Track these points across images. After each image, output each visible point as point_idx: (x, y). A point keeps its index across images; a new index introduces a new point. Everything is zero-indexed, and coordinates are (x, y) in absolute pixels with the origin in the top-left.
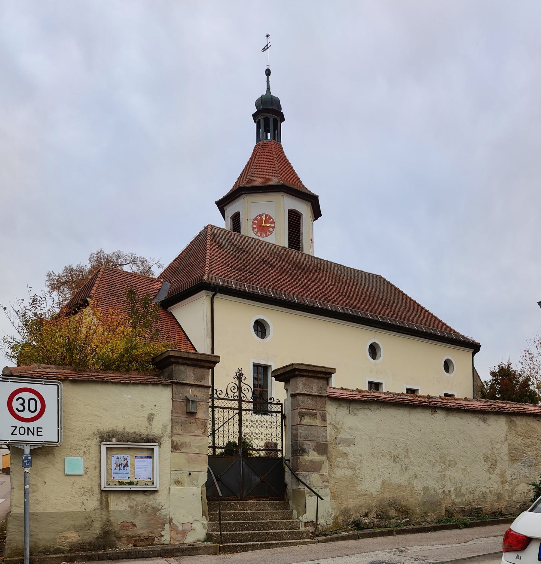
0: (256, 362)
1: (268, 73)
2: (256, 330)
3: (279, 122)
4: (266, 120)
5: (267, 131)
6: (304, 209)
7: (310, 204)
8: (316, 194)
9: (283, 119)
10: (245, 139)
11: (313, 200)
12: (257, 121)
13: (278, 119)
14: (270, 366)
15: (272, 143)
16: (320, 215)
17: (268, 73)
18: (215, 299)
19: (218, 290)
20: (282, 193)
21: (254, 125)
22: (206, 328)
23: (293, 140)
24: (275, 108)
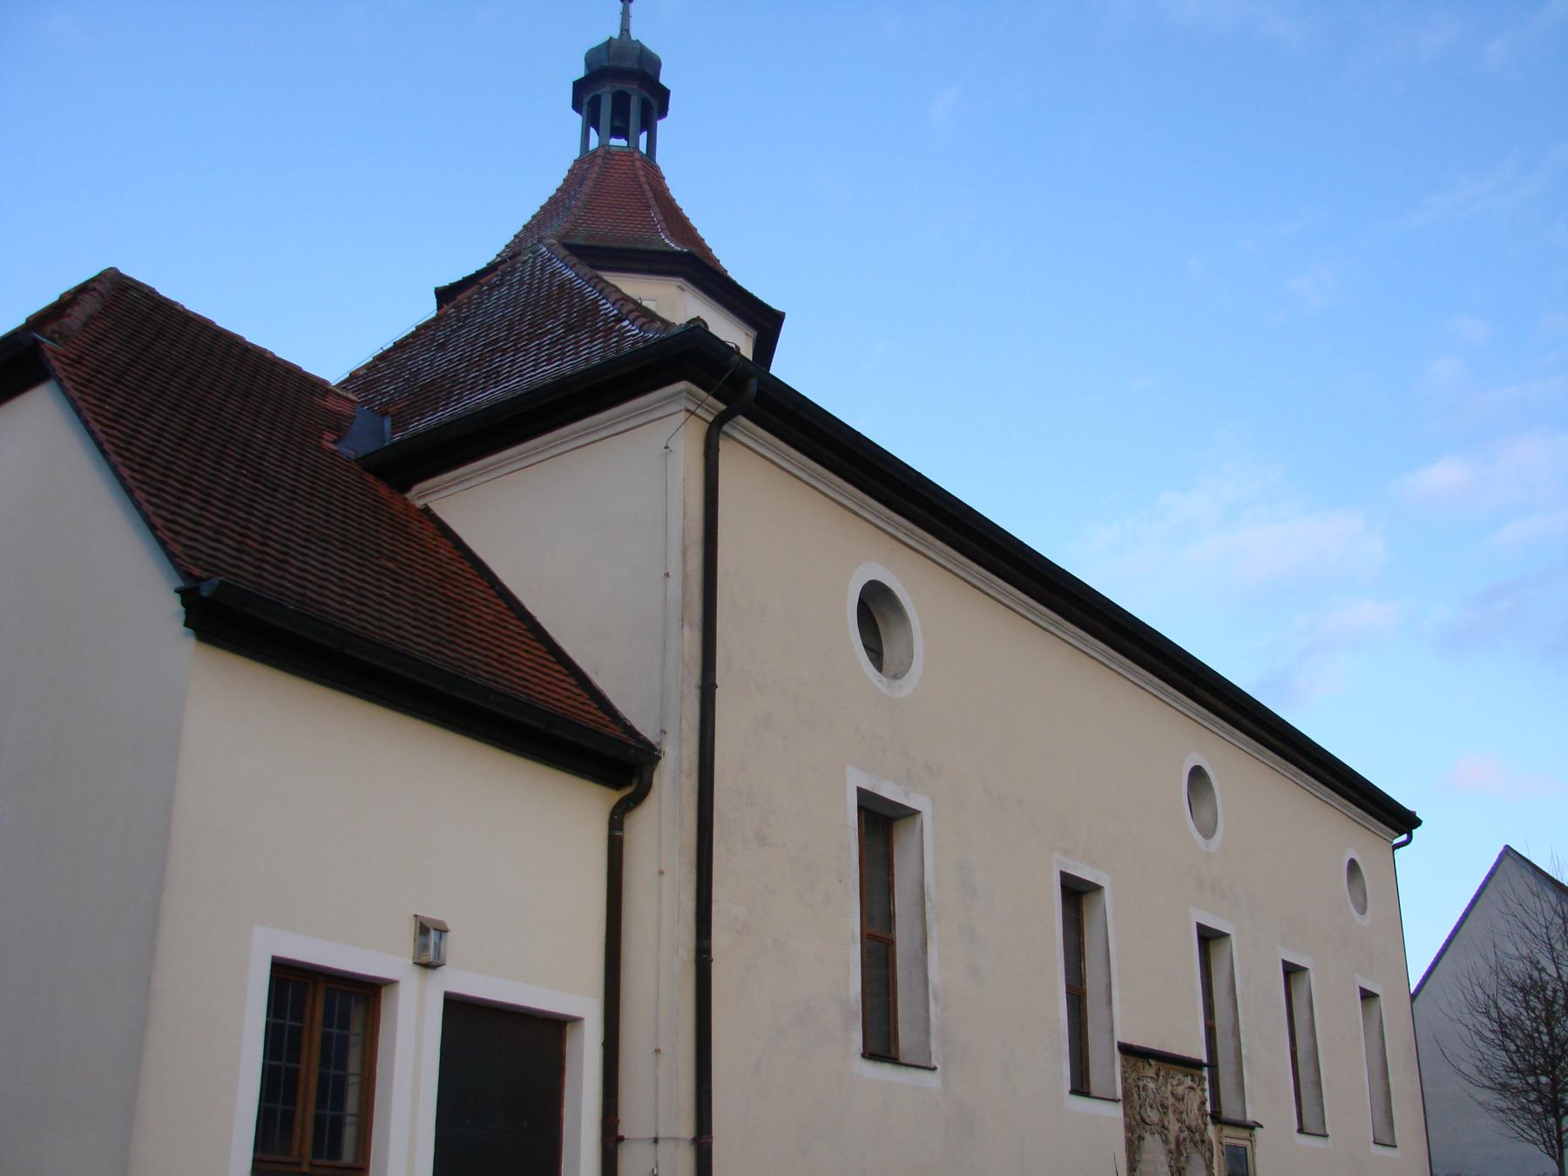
3: (655, 113)
4: (621, 105)
7: (753, 334)
8: (776, 305)
9: (663, 113)
12: (586, 100)
13: (655, 103)
14: (913, 813)
20: (680, 281)
24: (650, 71)
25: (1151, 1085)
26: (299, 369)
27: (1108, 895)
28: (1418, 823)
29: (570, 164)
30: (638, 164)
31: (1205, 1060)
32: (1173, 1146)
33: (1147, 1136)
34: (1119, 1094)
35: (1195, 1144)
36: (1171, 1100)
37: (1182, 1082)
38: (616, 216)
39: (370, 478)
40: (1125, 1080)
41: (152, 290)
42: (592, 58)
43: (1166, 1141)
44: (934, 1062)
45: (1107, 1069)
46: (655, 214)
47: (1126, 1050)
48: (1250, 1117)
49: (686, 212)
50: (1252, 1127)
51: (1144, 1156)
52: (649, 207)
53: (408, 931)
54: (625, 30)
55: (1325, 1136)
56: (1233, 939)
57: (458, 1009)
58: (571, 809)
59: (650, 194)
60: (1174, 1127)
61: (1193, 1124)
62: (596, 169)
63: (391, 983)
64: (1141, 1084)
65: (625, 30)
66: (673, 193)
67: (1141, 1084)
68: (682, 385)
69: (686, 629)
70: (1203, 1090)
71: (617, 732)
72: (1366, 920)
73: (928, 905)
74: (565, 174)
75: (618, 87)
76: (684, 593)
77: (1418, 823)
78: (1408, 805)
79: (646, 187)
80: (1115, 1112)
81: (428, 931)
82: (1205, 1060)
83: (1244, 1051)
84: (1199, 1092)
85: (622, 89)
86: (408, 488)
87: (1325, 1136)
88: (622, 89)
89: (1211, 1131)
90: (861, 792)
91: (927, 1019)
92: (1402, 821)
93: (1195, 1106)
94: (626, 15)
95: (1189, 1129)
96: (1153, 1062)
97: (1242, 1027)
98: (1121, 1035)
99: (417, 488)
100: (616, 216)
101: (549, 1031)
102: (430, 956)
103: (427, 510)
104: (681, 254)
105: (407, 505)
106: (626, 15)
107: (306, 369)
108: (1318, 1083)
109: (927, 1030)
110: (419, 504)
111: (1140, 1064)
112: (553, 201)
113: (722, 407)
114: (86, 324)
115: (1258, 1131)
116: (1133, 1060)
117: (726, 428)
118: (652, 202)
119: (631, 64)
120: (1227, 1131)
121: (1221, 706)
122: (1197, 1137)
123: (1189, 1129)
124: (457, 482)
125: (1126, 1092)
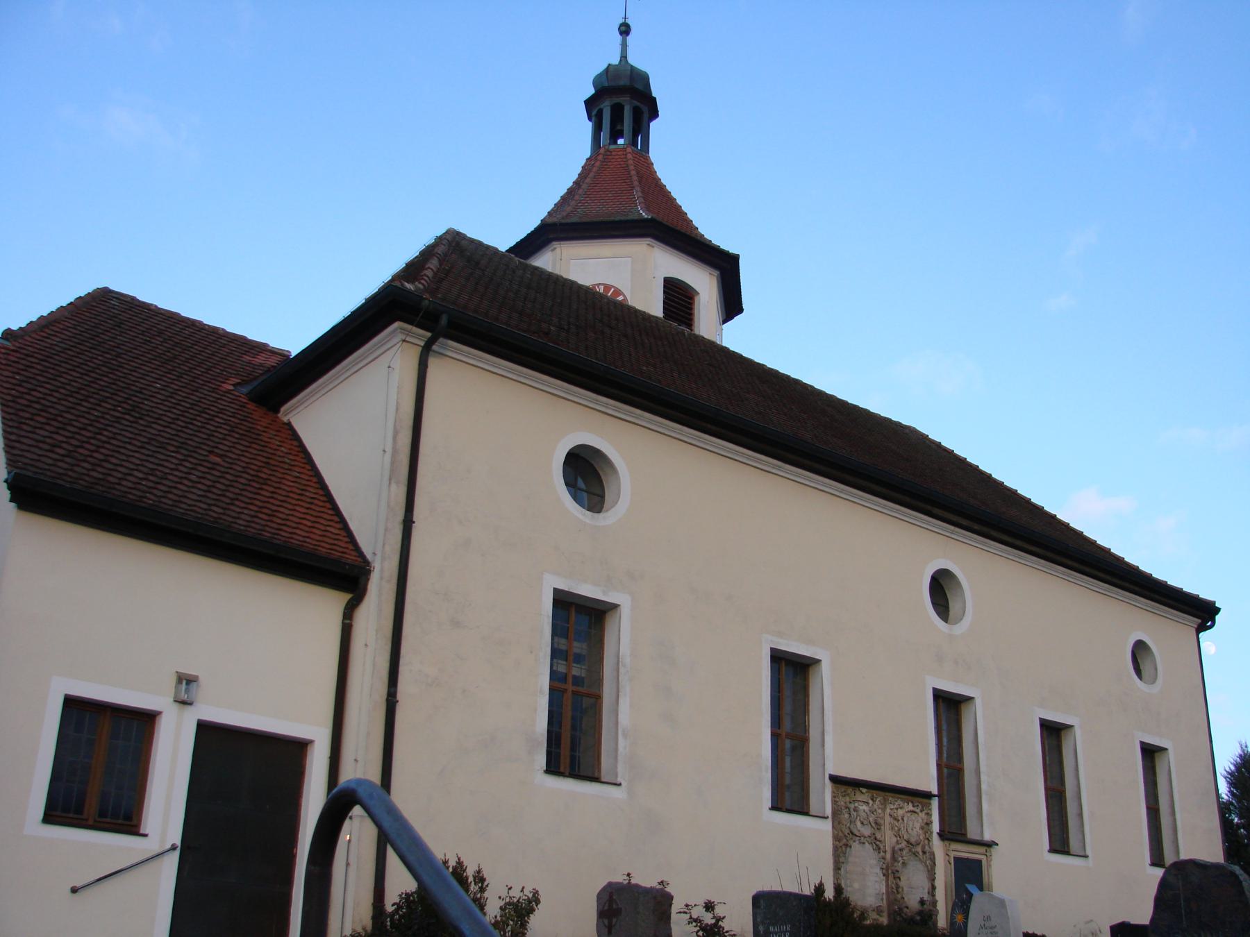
0: (563, 586)
1: (625, 30)
2: (570, 484)
3: (646, 116)
4: (617, 112)
5: (615, 134)
6: (703, 282)
7: (716, 273)
8: (733, 251)
9: (654, 114)
10: (570, 146)
11: (726, 267)
12: (594, 113)
13: (645, 109)
14: (615, 607)
15: (629, 150)
16: (740, 310)
17: (625, 30)
18: (434, 365)
19: (444, 320)
20: (648, 241)
21: (589, 126)
22: (389, 449)
23: (678, 157)
24: (639, 86)
25: (864, 807)
26: (245, 338)
27: (825, 667)
28: (1217, 610)
29: (583, 162)
30: (629, 156)
31: (935, 791)
32: (888, 856)
33: (856, 846)
34: (829, 812)
35: (915, 854)
36: (888, 819)
37: (904, 808)
38: (621, 196)
39: (252, 406)
40: (834, 802)
41: (133, 299)
42: (595, 83)
43: (878, 849)
44: (619, 780)
45: (822, 795)
46: (637, 193)
47: (835, 780)
48: (987, 837)
49: (668, 188)
50: (990, 845)
51: (850, 859)
52: (633, 188)
53: (174, 679)
54: (624, 57)
55: (1086, 857)
56: (978, 702)
57: (204, 729)
58: (319, 608)
59: (635, 178)
60: (889, 839)
61: (913, 840)
62: (598, 164)
63: (159, 713)
64: (852, 806)
65: (624, 57)
66: (659, 174)
67: (852, 806)
68: (396, 325)
69: (394, 486)
70: (929, 815)
71: (351, 557)
72: (1156, 689)
73: (622, 670)
74: (579, 170)
75: (616, 100)
76: (393, 463)
77: (1217, 610)
78: (1205, 594)
79: (633, 173)
80: (827, 826)
81: (186, 681)
82: (935, 791)
83: (984, 787)
84: (922, 815)
85: (623, 104)
86: (277, 411)
87: (1086, 857)
88: (623, 104)
89: (937, 845)
90: (555, 590)
91: (616, 750)
92: (1202, 613)
93: (918, 826)
94: (624, 46)
95: (908, 842)
96: (864, 790)
97: (983, 768)
98: (831, 769)
99: (283, 409)
100: (621, 196)
101: (299, 747)
102: (184, 697)
103: (289, 424)
104: (647, 220)
105: (276, 420)
106: (624, 46)
107: (250, 337)
108: (1080, 815)
109: (616, 758)
110: (285, 419)
111: (850, 790)
112: (570, 192)
113: (429, 334)
114: (46, 326)
115: (994, 850)
116: (843, 788)
117: (434, 347)
118: (636, 183)
119: (624, 82)
120: (955, 846)
121: (965, 522)
122: (919, 849)
123: (908, 842)
124: (301, 403)
125: (836, 813)
